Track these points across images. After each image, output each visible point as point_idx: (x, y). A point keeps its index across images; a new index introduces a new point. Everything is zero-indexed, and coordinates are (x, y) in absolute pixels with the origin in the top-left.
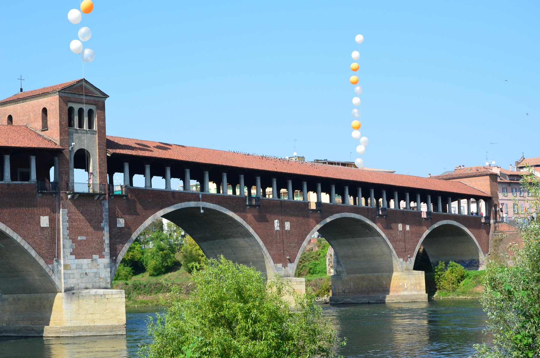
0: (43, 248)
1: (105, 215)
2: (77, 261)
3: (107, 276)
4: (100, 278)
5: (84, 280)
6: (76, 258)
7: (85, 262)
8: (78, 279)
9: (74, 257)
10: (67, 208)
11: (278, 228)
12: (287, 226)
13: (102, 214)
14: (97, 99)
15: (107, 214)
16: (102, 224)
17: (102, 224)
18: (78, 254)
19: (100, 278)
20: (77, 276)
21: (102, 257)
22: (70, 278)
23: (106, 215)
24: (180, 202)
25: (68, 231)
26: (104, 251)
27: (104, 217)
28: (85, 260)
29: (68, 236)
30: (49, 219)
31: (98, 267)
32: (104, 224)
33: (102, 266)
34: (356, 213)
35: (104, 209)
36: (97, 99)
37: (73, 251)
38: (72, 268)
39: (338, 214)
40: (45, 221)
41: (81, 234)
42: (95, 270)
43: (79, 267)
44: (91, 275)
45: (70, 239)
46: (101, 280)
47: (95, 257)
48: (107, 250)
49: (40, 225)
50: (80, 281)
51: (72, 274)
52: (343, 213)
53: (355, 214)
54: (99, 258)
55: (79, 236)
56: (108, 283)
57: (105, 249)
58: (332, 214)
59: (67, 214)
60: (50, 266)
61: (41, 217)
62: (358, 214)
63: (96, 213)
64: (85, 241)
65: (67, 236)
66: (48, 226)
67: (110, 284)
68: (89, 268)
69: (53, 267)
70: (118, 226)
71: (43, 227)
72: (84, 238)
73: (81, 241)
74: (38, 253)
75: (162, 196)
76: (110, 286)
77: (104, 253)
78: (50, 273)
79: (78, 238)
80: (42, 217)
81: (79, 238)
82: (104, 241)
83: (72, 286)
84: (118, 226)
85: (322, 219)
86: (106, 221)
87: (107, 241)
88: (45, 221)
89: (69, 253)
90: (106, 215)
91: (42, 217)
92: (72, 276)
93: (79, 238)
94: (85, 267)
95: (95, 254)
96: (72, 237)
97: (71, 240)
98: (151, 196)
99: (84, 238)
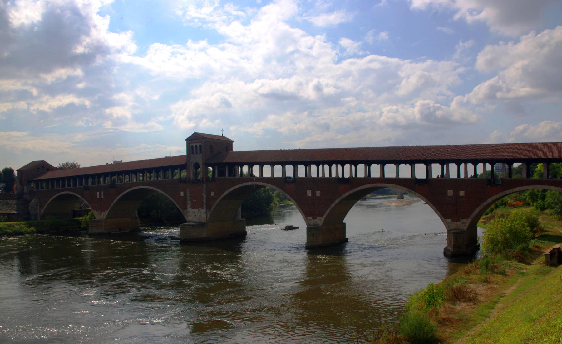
2: (193, 210)
7: (196, 211)
9: (191, 208)
11: (310, 195)
12: (318, 194)
15: (205, 190)
16: (203, 195)
18: (193, 207)
40: (182, 194)
42: (200, 214)
44: (198, 216)
47: (200, 208)
48: (205, 206)
60: (184, 212)
70: (212, 195)
72: (195, 200)
78: (184, 214)
81: (194, 201)
83: (190, 220)
84: (212, 195)
87: (205, 202)
88: (182, 194)
93: (194, 201)
94: (196, 213)
99: (195, 200)
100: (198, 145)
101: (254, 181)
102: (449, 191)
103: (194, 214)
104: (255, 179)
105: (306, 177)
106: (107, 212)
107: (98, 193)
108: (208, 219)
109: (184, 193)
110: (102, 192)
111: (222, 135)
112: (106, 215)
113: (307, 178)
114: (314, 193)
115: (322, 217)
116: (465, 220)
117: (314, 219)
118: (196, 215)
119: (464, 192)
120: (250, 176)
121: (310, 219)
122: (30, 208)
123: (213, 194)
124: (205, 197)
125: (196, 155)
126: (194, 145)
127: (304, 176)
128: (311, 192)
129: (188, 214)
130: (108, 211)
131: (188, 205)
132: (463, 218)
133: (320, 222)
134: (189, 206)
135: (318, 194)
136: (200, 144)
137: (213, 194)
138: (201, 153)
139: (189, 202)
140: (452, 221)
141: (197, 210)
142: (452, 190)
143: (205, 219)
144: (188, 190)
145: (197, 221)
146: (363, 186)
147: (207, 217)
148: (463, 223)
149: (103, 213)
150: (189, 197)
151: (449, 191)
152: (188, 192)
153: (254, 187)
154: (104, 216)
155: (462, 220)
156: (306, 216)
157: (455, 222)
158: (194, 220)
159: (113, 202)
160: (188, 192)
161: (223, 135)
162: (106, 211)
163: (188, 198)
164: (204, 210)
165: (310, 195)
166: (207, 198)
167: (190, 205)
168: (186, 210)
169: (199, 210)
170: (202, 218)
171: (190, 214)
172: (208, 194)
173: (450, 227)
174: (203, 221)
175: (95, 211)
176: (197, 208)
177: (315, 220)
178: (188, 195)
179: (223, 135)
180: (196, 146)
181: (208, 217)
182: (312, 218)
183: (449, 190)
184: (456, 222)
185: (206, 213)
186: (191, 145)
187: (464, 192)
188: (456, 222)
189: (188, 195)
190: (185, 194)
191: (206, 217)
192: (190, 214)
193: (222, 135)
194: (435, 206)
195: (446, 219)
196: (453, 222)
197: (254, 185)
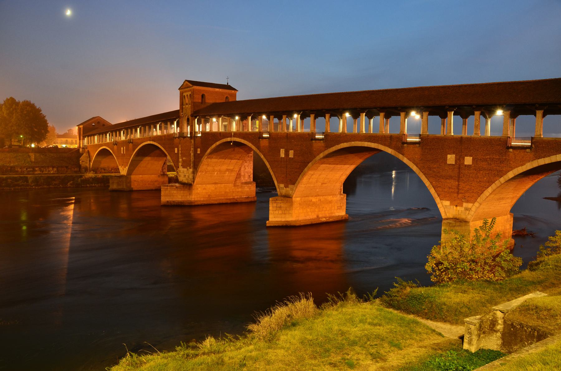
7: (185, 169)
21: (190, 168)
34: (371, 142)
39: (345, 143)
42: (188, 175)
52: (353, 142)
53: (369, 143)
58: (339, 143)
62: (374, 142)
70: (198, 153)
84: (198, 153)
85: (326, 149)
102: (449, 156)
103: (183, 174)
106: (127, 168)
107: (122, 148)
110: (125, 147)
111: (227, 84)
112: (127, 169)
114: (287, 154)
115: (294, 186)
116: (470, 205)
117: (286, 187)
119: (471, 158)
121: (281, 187)
122: (80, 161)
123: (199, 151)
128: (284, 152)
130: (128, 167)
132: (468, 202)
133: (291, 191)
135: (291, 154)
137: (199, 151)
139: (180, 160)
140: (451, 204)
141: (186, 169)
142: (454, 155)
146: (339, 145)
148: (467, 209)
151: (449, 156)
152: (180, 149)
153: (231, 144)
155: (465, 205)
157: (455, 207)
160: (180, 149)
161: (228, 83)
164: (191, 170)
166: (194, 155)
169: (187, 169)
172: (195, 151)
173: (448, 214)
175: (120, 166)
179: (228, 83)
180: (187, 95)
183: (450, 154)
184: (456, 206)
187: (471, 158)
188: (456, 206)
189: (180, 152)
193: (227, 84)
194: (428, 179)
195: (442, 201)
196: (452, 207)
197: (232, 141)
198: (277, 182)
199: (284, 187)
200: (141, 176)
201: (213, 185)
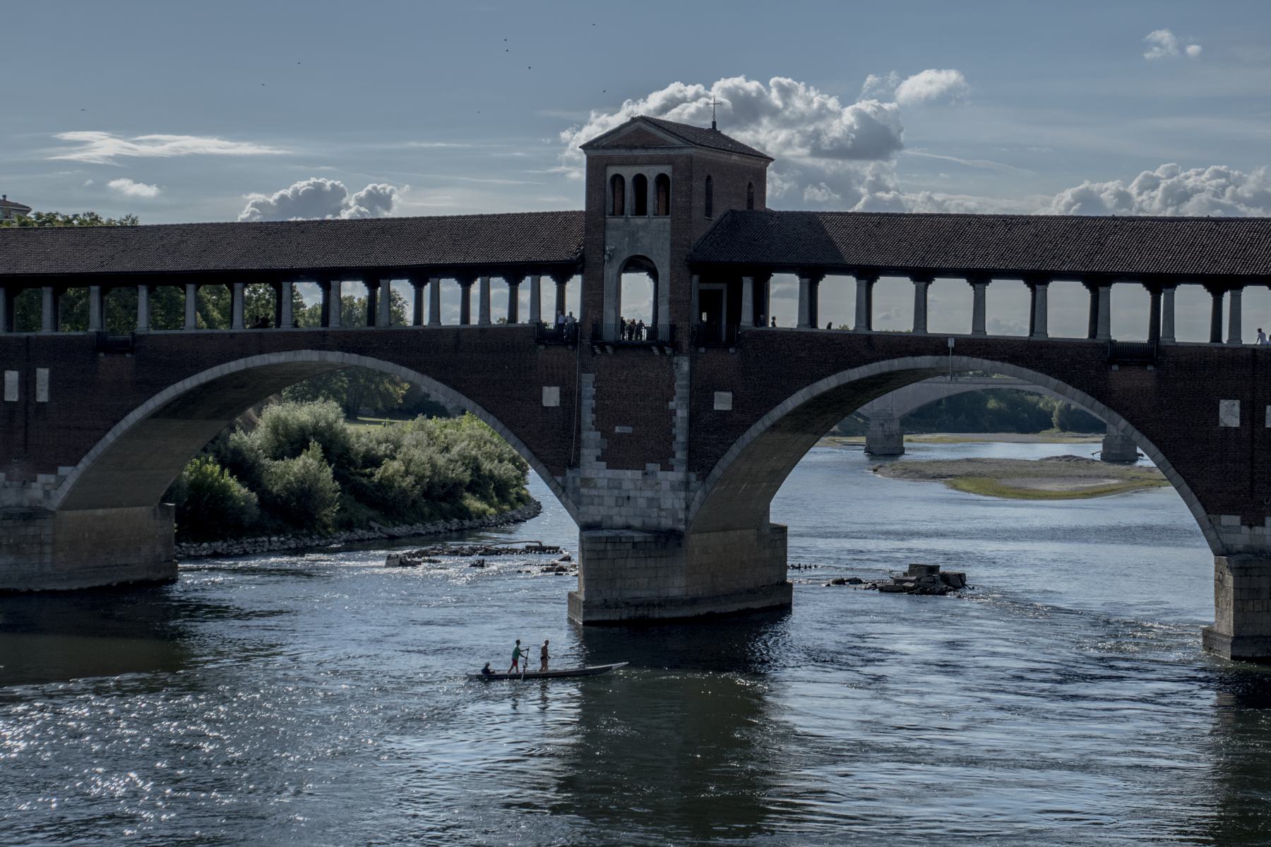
0: (546, 444)
1: (680, 386)
2: (610, 473)
3: (677, 506)
4: (661, 510)
5: (624, 511)
6: (608, 468)
8: (610, 507)
9: (604, 464)
10: (593, 372)
11: (1234, 422)
13: (673, 385)
14: (672, 153)
16: (672, 405)
17: (670, 403)
18: (612, 459)
19: (661, 510)
20: (611, 501)
21: (667, 467)
22: (592, 504)
23: (681, 387)
24: (888, 358)
25: (594, 415)
26: (674, 457)
27: (678, 390)
28: (629, 473)
29: (593, 424)
30: (561, 392)
31: (657, 487)
32: (677, 404)
33: (666, 486)
35: (677, 375)
36: (672, 153)
37: (602, 454)
38: (599, 485)
40: (551, 397)
41: (623, 422)
42: (649, 494)
43: (615, 485)
44: (642, 502)
45: (596, 430)
46: (664, 514)
48: (680, 455)
49: (541, 403)
50: (615, 511)
51: (598, 496)
54: (662, 470)
55: (617, 425)
56: (680, 520)
57: (674, 453)
59: (594, 383)
60: (559, 479)
61: (544, 387)
63: (658, 382)
64: (629, 435)
65: (591, 425)
66: (558, 405)
67: (683, 522)
68: (636, 489)
69: (565, 481)
70: (717, 407)
71: (547, 408)
72: (628, 430)
73: (621, 435)
74: (535, 454)
75: (837, 344)
76: (684, 527)
77: (672, 461)
79: (614, 429)
80: (546, 389)
81: (618, 429)
82: (674, 438)
83: (598, 518)
84: (717, 407)
86: (681, 398)
87: (681, 438)
88: (551, 397)
89: (594, 459)
90: (681, 387)
91: (546, 389)
92: (596, 500)
93: (618, 429)
94: (627, 485)
95: (652, 462)
96: (603, 426)
97: (599, 433)
98: (807, 345)
99: (628, 430)
100: (651, 173)
101: (947, 354)
103: (616, 492)
104: (951, 344)
105: (1217, 345)
107: (12, 377)
108: (691, 516)
109: (563, 395)
112: (67, 486)
113: (1223, 348)
118: (629, 498)
120: (756, 325)
123: (723, 402)
124: (682, 413)
125: (640, 221)
126: (628, 173)
127: (1203, 336)
129: (584, 491)
131: (584, 452)
134: (589, 454)
136: (666, 170)
137: (723, 402)
138: (667, 213)
139: (591, 438)
141: (639, 473)
143: (681, 515)
144: (588, 379)
145: (637, 522)
147: (688, 508)
149: (42, 478)
150: (594, 411)
154: (47, 494)
156: (1208, 513)
158: (619, 521)
159: (116, 421)
162: (63, 470)
163: (588, 418)
165: (1234, 422)
166: (692, 418)
167: (599, 452)
168: (569, 474)
170: (660, 509)
171: (594, 492)
174: (667, 523)
176: (637, 463)
177: (1258, 530)
178: (588, 403)
180: (640, 181)
181: (695, 506)
182: (1243, 524)
185: (686, 485)
186: (612, 171)
189: (588, 403)
190: (570, 397)
191: (684, 505)
192: (594, 492)
198: (1206, 510)
199: (1239, 524)
200: (100, 512)
201: (721, 534)
